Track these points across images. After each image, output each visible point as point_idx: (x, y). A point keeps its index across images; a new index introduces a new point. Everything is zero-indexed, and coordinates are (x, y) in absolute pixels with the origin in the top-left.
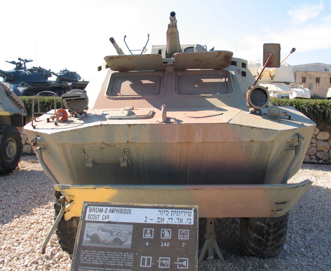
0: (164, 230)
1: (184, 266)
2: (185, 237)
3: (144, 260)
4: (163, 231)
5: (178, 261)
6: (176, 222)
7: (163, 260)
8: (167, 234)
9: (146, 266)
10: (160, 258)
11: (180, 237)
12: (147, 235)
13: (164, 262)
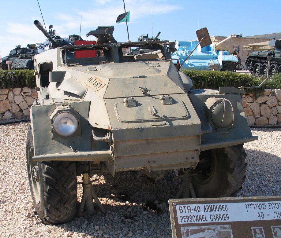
0: (275, 228)
4: (274, 228)
6: (274, 217)
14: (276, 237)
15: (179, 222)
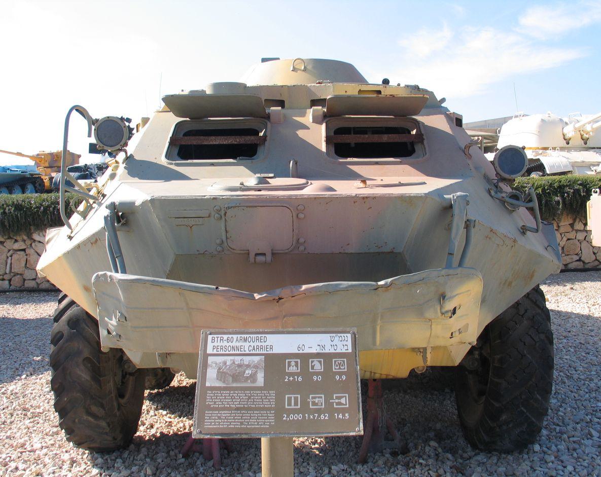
1: (343, 405)
2: (343, 367)
3: (289, 399)
4: (312, 362)
5: (335, 398)
7: (315, 398)
8: (318, 366)
9: (293, 407)
10: (311, 396)
11: (335, 368)
12: (291, 368)
13: (316, 400)
14: (313, 371)
15: (209, 351)
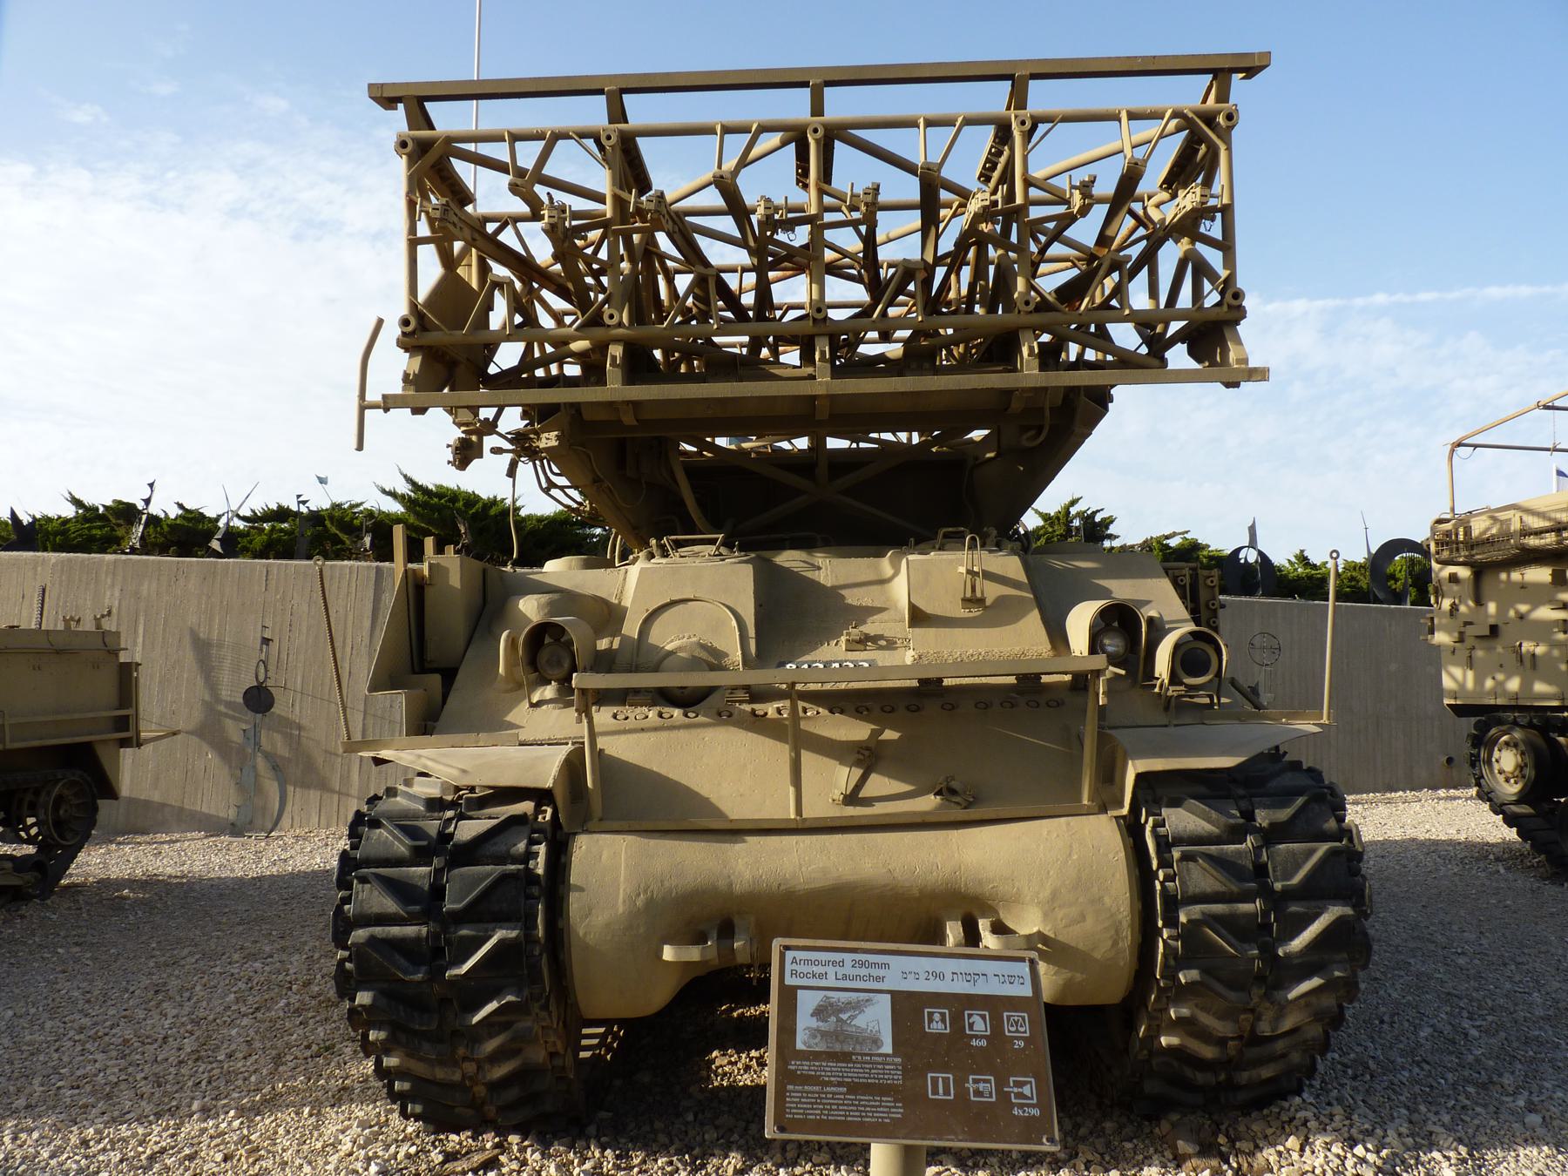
1: (1026, 1097)
3: (935, 1081)
4: (970, 1016)
8: (979, 1024)
11: (1008, 1030)
12: (934, 1025)
13: (981, 1086)
